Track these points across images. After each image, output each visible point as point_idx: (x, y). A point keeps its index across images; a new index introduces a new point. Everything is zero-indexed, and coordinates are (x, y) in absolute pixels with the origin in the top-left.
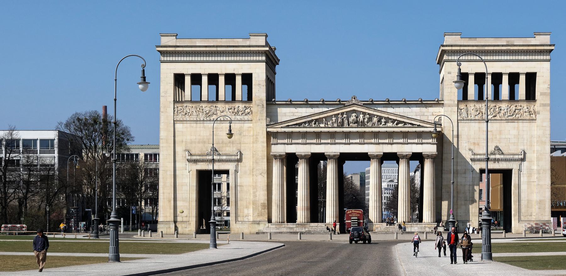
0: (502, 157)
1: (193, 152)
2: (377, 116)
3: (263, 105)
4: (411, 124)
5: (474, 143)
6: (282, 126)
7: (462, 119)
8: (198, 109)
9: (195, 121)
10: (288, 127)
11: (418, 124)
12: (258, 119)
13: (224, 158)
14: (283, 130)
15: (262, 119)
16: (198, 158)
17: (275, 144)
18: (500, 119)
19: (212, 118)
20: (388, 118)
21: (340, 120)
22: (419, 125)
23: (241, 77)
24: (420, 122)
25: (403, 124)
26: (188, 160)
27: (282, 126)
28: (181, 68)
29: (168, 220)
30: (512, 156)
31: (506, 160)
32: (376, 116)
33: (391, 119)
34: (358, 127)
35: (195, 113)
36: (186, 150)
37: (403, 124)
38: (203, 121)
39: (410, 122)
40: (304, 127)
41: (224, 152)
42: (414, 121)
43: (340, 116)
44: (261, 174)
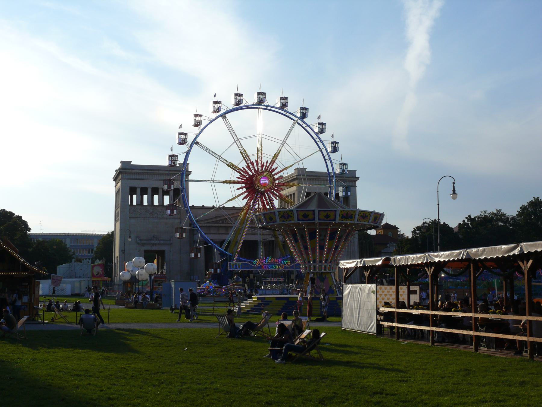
6: (206, 222)
8: (145, 210)
10: (209, 223)
13: (162, 242)
14: (206, 225)
16: (145, 242)
19: (154, 216)
27: (206, 222)
28: (134, 183)
36: (137, 237)
38: (149, 218)
40: (219, 223)
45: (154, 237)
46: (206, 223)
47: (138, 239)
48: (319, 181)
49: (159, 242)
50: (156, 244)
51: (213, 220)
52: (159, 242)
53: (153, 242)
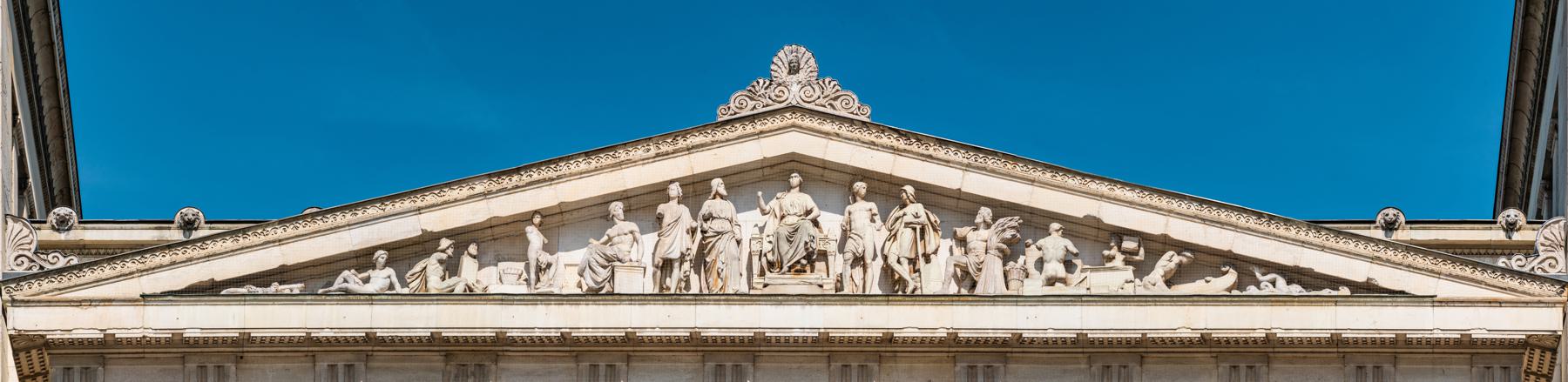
2: (1002, 209)
4: (1293, 274)
20: (1094, 224)
24: (1375, 259)
25: (1231, 277)
32: (985, 213)
33: (1119, 234)
37: (1231, 277)
42: (1323, 248)
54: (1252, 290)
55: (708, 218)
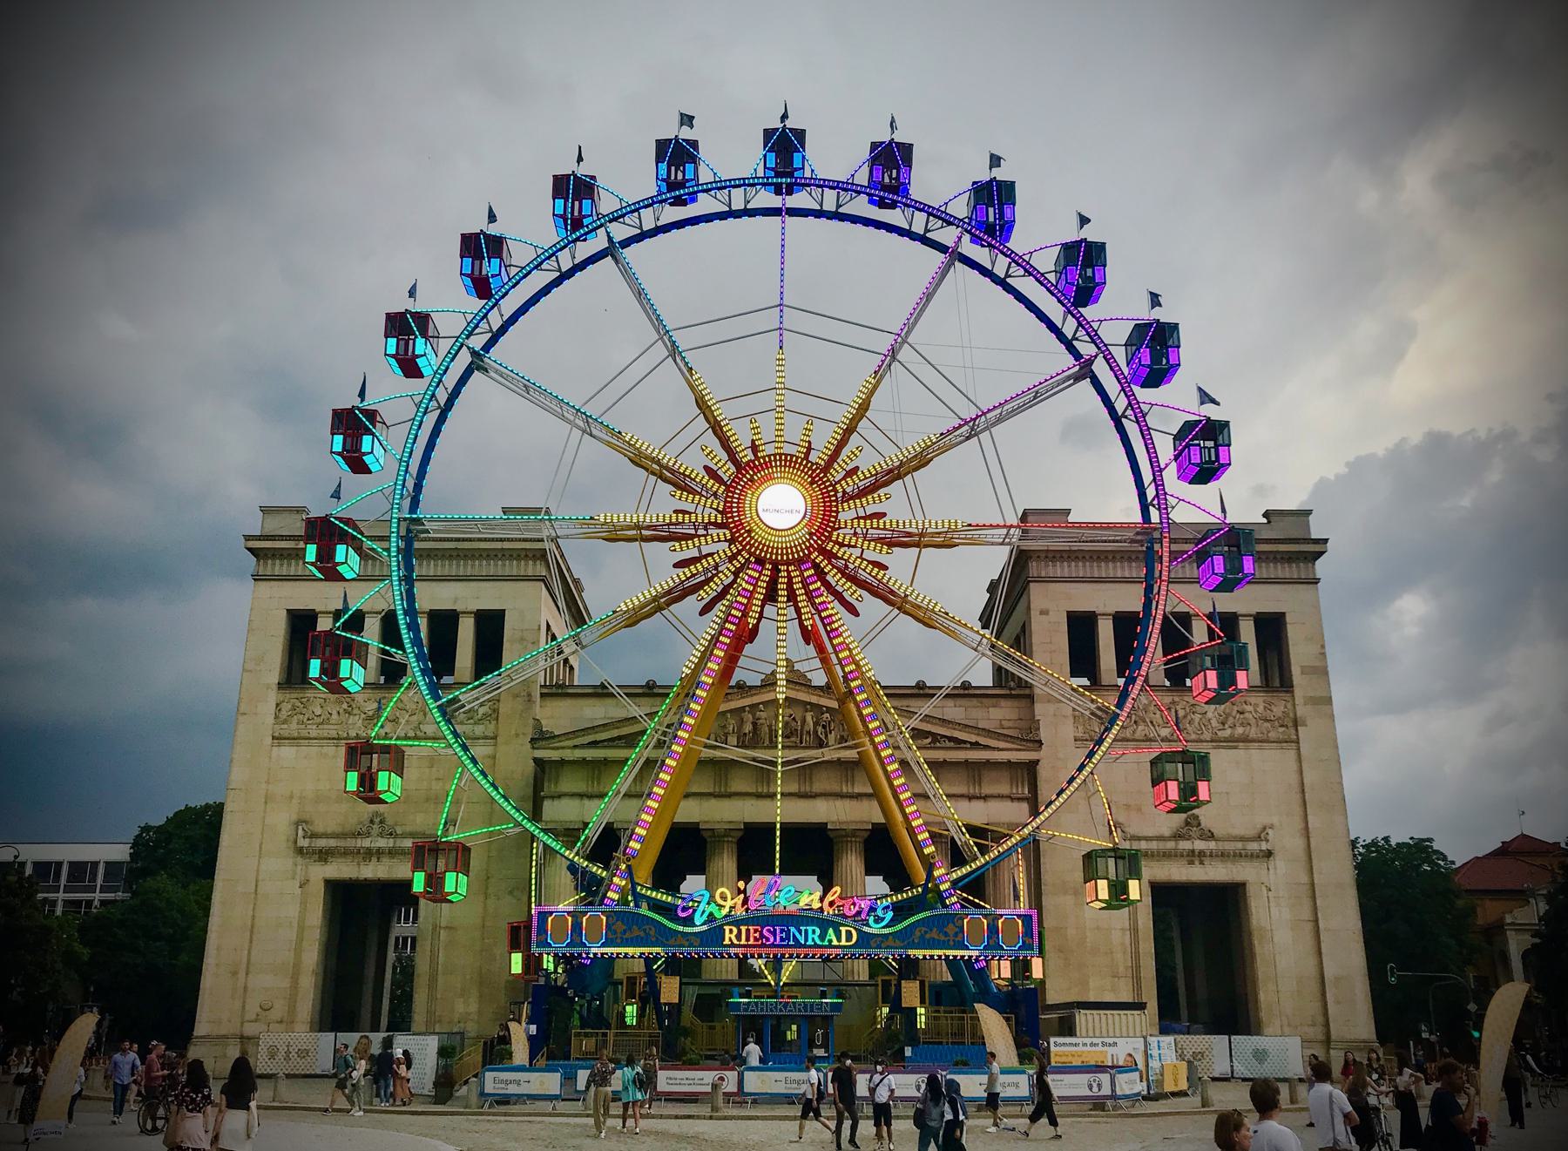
0: (1212, 845)
1: (320, 829)
3: (529, 695)
4: (951, 739)
5: (1128, 806)
7: (1087, 736)
8: (345, 706)
9: (333, 739)
10: (594, 744)
11: (973, 738)
12: (513, 732)
15: (524, 734)
16: (332, 843)
17: (553, 798)
18: (1193, 737)
21: (748, 728)
22: (977, 744)
23: (473, 620)
25: (929, 740)
26: (300, 851)
29: (223, 1032)
30: (1239, 845)
31: (1223, 856)
34: (796, 747)
35: (335, 716)
36: (297, 823)
37: (929, 740)
39: (948, 733)
41: (408, 829)
43: (748, 717)
44: (511, 893)
45: (372, 822)
46: (582, 746)
47: (300, 832)
48: (1134, 564)
49: (391, 843)
50: (379, 853)
51: (615, 733)
52: (391, 843)
53: (366, 843)
54: (938, 744)
55: (759, 719)
